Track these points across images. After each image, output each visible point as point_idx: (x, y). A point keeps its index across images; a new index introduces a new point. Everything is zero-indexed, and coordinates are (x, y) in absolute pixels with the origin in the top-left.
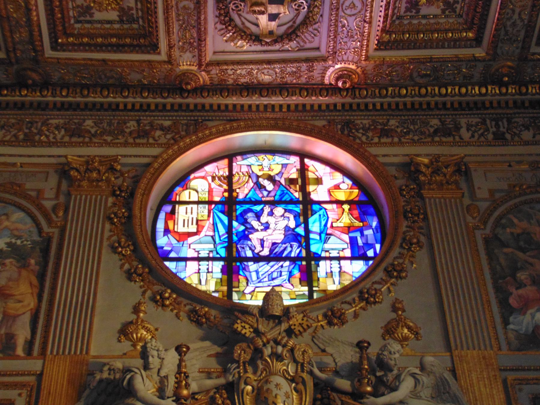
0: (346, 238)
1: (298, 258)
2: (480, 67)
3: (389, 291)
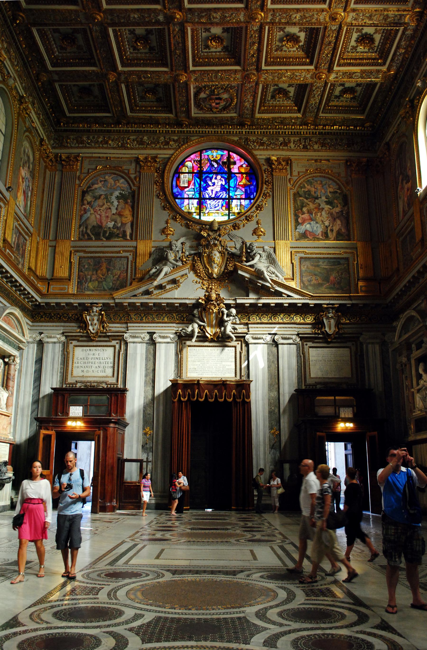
0: (244, 190)
1: (225, 199)
2: (300, 120)
3: (256, 216)
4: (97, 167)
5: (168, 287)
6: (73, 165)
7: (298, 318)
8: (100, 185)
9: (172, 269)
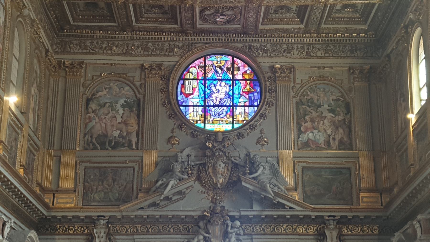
0: (247, 97)
4: (101, 74)
5: (174, 198)
6: (77, 72)
7: (300, 229)
8: (105, 92)
9: (178, 181)
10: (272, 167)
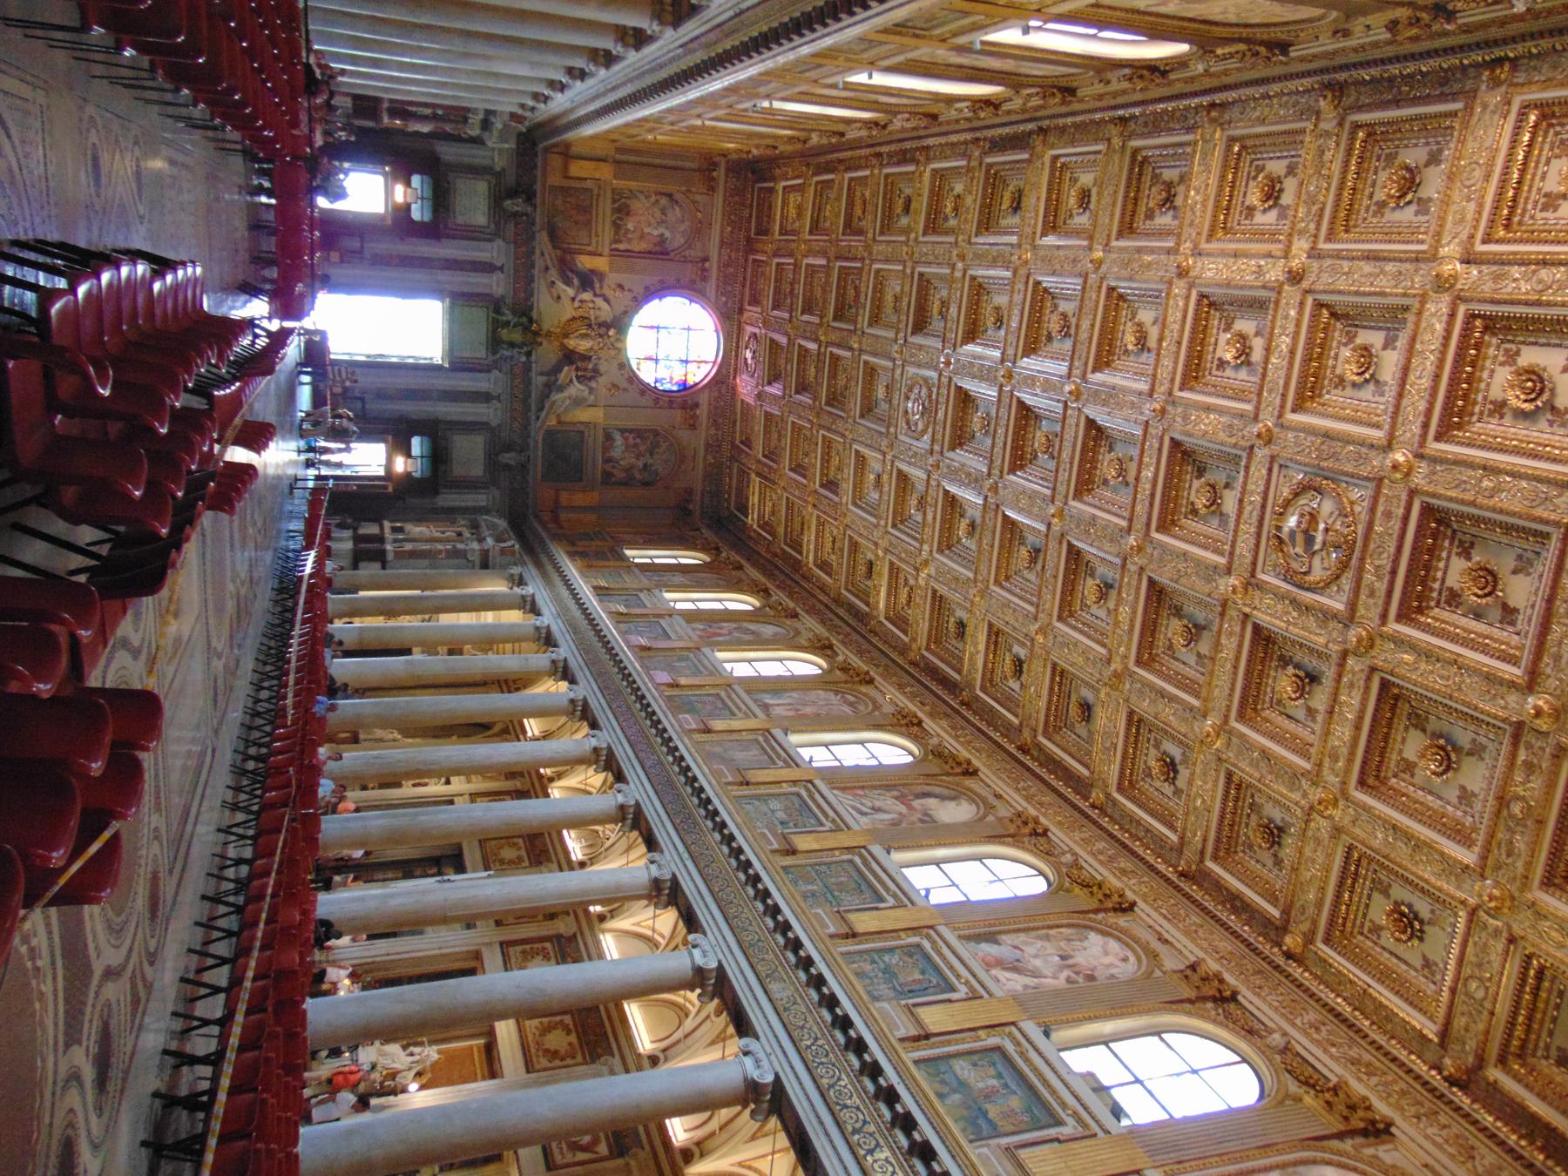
10: (585, 399)
